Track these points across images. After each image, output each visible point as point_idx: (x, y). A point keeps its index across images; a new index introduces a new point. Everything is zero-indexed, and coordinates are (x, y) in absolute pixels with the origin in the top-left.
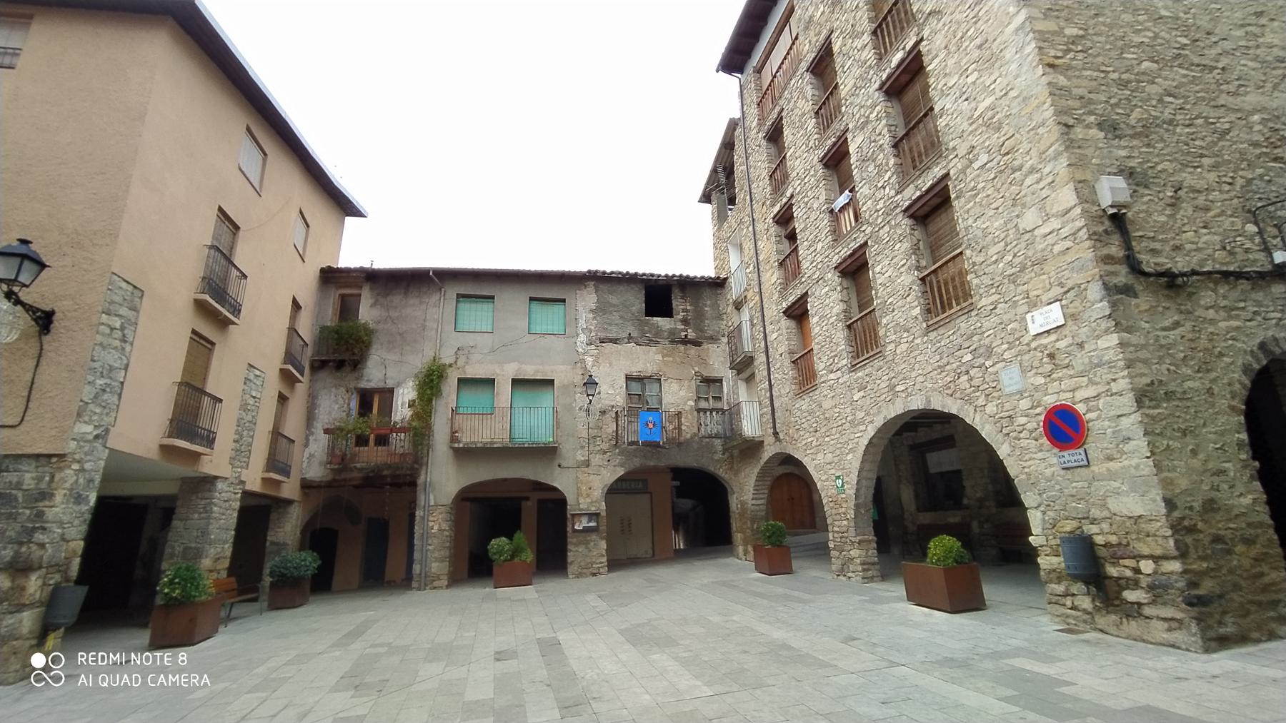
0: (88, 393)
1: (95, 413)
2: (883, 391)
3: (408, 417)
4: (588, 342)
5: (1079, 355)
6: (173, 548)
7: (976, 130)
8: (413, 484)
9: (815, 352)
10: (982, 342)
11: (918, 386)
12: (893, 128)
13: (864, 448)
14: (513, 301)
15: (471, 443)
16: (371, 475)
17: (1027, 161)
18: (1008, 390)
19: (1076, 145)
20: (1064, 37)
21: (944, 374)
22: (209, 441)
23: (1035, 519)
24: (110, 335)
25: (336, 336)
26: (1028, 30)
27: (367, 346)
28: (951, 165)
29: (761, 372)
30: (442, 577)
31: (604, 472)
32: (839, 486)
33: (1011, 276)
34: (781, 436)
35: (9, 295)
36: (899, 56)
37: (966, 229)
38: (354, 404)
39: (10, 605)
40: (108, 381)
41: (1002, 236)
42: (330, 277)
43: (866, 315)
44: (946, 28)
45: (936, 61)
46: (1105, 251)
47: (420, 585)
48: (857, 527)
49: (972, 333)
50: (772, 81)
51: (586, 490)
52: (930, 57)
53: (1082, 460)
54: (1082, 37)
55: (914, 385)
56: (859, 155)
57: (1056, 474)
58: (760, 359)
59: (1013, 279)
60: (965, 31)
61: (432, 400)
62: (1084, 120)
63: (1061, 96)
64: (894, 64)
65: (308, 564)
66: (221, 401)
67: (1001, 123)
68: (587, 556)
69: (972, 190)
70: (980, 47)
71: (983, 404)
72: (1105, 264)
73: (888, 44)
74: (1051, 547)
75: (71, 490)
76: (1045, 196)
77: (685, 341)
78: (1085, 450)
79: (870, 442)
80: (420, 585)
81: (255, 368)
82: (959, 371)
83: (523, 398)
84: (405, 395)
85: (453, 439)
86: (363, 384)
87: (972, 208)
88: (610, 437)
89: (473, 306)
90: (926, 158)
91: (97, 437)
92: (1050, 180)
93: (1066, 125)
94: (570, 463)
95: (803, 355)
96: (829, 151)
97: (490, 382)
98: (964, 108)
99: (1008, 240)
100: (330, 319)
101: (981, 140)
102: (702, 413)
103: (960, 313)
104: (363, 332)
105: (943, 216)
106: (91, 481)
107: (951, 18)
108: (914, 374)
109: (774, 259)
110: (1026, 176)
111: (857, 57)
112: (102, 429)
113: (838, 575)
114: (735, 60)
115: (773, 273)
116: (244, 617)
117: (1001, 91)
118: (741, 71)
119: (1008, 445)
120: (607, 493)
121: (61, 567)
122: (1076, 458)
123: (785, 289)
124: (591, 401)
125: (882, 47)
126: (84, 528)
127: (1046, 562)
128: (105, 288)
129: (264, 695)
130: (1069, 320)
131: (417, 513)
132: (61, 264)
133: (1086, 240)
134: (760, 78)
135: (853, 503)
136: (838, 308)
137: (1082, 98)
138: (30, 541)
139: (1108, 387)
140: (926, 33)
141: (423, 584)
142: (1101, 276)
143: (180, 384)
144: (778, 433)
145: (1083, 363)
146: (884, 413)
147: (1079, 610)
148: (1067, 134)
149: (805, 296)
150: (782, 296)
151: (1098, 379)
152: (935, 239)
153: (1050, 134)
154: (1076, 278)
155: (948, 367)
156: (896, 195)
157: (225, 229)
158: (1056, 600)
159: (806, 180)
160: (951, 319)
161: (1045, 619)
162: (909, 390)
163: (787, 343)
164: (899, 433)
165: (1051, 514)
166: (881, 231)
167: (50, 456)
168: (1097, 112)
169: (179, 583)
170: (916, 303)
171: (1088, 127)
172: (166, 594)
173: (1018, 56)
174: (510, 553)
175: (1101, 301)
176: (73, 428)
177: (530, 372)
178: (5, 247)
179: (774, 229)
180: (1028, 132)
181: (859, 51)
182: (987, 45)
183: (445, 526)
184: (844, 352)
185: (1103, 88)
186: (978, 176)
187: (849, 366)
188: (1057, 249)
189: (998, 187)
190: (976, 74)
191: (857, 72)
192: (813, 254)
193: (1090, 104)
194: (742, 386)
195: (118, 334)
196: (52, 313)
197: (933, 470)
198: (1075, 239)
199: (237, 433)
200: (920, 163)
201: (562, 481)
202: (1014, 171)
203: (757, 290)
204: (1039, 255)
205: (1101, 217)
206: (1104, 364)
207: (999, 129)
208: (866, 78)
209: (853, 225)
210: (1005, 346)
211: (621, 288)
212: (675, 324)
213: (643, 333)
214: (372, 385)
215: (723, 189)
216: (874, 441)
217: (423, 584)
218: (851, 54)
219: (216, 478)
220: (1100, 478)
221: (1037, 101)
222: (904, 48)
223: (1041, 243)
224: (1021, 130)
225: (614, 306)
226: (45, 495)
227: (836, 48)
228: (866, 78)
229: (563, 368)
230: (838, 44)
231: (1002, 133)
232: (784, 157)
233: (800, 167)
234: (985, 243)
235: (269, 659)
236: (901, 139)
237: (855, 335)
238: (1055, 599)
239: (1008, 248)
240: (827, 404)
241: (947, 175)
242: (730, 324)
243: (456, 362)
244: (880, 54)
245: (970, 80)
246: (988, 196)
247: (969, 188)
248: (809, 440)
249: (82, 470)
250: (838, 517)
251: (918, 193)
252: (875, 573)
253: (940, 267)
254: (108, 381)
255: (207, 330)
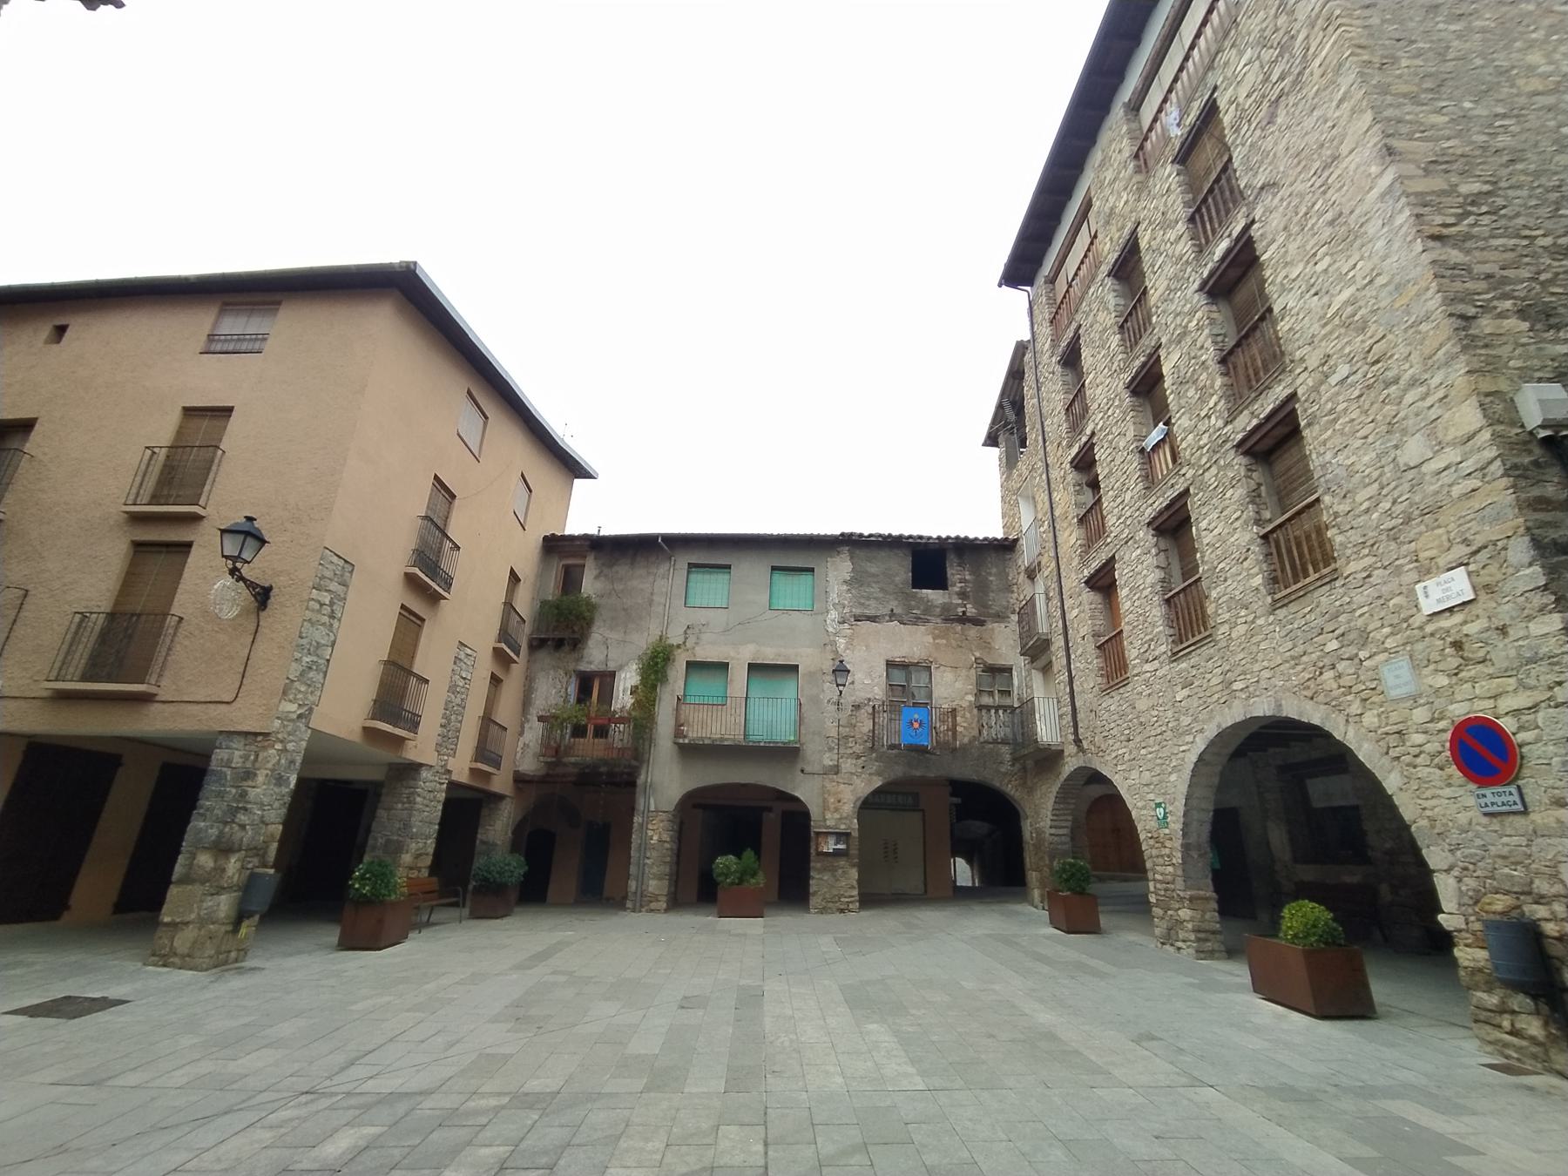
0: (294, 670)
1: (300, 691)
2: (1214, 689)
3: (629, 705)
4: (841, 620)
5: (1501, 645)
6: (376, 839)
7: (1331, 333)
8: (631, 784)
9: (1125, 635)
10: (1352, 624)
11: (1263, 684)
12: (1220, 339)
13: (1192, 766)
14: (752, 571)
15: (699, 739)
16: (587, 771)
17: (1405, 371)
18: (1394, 693)
19: (1481, 344)
20: (1458, 196)
21: (1299, 668)
22: (414, 724)
23: (1447, 889)
24: (319, 611)
25: (556, 611)
26: (1398, 194)
27: (589, 623)
28: (1299, 381)
29: (1059, 661)
30: (660, 898)
31: (857, 781)
32: (1161, 817)
33: (1391, 530)
34: (1085, 744)
35: (233, 571)
36: (1224, 245)
37: (1323, 466)
38: (573, 689)
39: (211, 886)
40: (315, 659)
41: (1375, 474)
42: (555, 545)
43: (1190, 585)
44: (1285, 203)
45: (1273, 247)
46: (1536, 492)
47: (635, 905)
48: (1186, 878)
49: (1338, 611)
50: (1067, 291)
51: (833, 803)
52: (1264, 243)
53: (1515, 803)
54: (1488, 193)
55: (1257, 682)
56: (1176, 376)
57: (1474, 821)
58: (1058, 643)
59: (1393, 535)
60: (1310, 204)
61: (656, 686)
62: (1495, 308)
63: (1453, 278)
64: (1217, 257)
65: (512, 869)
66: (427, 681)
67: (1366, 322)
68: (833, 887)
69: (1330, 412)
70: (1331, 223)
71: (1359, 712)
72: (1535, 510)
73: (1209, 232)
74: (1474, 933)
75: (273, 770)
76: (1434, 417)
77: (963, 619)
78: (1519, 788)
79: (1201, 758)
80: (635, 905)
81: (466, 646)
82: (1321, 664)
83: (760, 687)
84: (628, 680)
85: (678, 733)
86: (583, 667)
87: (1330, 438)
88: (866, 738)
89: (707, 577)
90: (1265, 374)
91: (300, 716)
92: (1440, 394)
93: (1463, 317)
94: (817, 768)
95: (1110, 639)
96: (1138, 373)
97: (723, 667)
98: (1313, 305)
99: (1384, 480)
100: (552, 591)
101: (1339, 347)
102: (984, 712)
103: (1319, 583)
104: (584, 608)
105: (1294, 450)
106: (292, 762)
107: (1290, 190)
108: (1256, 667)
109: (1074, 513)
110: (1405, 391)
111: (1170, 252)
112: (306, 708)
113: (1163, 944)
114: (1020, 271)
115: (1072, 532)
116: (443, 923)
117: (1365, 278)
118: (1030, 282)
119: (1399, 775)
120: (860, 808)
121: (258, 851)
122: (1504, 799)
123: (1086, 552)
124: (841, 692)
125: (1202, 235)
126: (284, 811)
127: (1468, 955)
128: (317, 563)
129: (423, 1015)
130: (1482, 593)
131: (635, 819)
132: (281, 539)
133: (1502, 476)
134: (1054, 289)
135: (1180, 841)
136: (1154, 576)
137: (1489, 276)
138: (233, 822)
139: (1549, 694)
140: (1258, 214)
141: (638, 904)
142: (1528, 529)
143: (387, 663)
144: (1080, 741)
145: (1507, 657)
146: (1218, 719)
147: (1523, 1038)
148: (1464, 329)
149: (1112, 560)
150: (1084, 563)
151: (1532, 682)
152: (1284, 481)
153: (1439, 331)
154: (1489, 533)
155: (1305, 659)
156: (1225, 426)
157: (441, 498)
158: (1484, 1018)
159: (1110, 413)
160: (1306, 592)
161: (1471, 1045)
162: (1251, 689)
163: (1090, 622)
164: (1239, 753)
165: (1470, 883)
166: (1206, 474)
167: (256, 734)
168: (1516, 294)
169: (369, 879)
170: (1256, 570)
171: (1502, 315)
172: (357, 889)
173: (1385, 230)
174: (738, 875)
175: (1530, 565)
176: (278, 706)
177: (770, 655)
178: (232, 525)
179: (1072, 476)
180: (1406, 330)
181: (1172, 244)
182: (1342, 220)
183: (666, 837)
184: (1162, 635)
185: (1527, 260)
186: (1338, 394)
187: (1169, 654)
188: (1456, 491)
189: (1366, 407)
190: (1327, 260)
191: (1170, 270)
192: (1121, 507)
193: (1505, 284)
194: (1037, 677)
195: (326, 610)
196: (270, 588)
197: (1318, 802)
198: (1484, 476)
199: (444, 716)
200: (1257, 381)
201: (805, 791)
202: (1388, 385)
203: (1052, 554)
204: (1430, 501)
205: (1525, 443)
206: (1542, 659)
207: (1363, 329)
208: (1183, 277)
209: (1171, 466)
210: (1386, 630)
211: (883, 554)
212: (950, 598)
213: (909, 609)
214: (593, 667)
215: (1013, 428)
216: (1206, 757)
217: (638, 904)
218: (1162, 249)
219: (421, 765)
220: (1546, 833)
221: (1416, 287)
222: (1229, 236)
223: (1432, 484)
224: (1395, 329)
225: (874, 575)
226: (249, 775)
227: (1143, 244)
228: (1183, 277)
229: (809, 651)
230: (1147, 238)
231: (1369, 334)
232: (1083, 385)
233: (1102, 396)
234: (1351, 485)
235: (443, 974)
236: (1231, 352)
237: (1177, 613)
238: (1483, 1015)
239: (1384, 492)
240: (1142, 704)
241: (1293, 397)
242: (1022, 597)
243: (684, 643)
244: (1200, 246)
245: (1319, 268)
246: (1353, 420)
247: (1326, 411)
248: (1120, 752)
249: (285, 750)
250: (1160, 860)
251: (1255, 422)
252: (1216, 946)
253: (1289, 520)
254: (315, 659)
255: (417, 606)
